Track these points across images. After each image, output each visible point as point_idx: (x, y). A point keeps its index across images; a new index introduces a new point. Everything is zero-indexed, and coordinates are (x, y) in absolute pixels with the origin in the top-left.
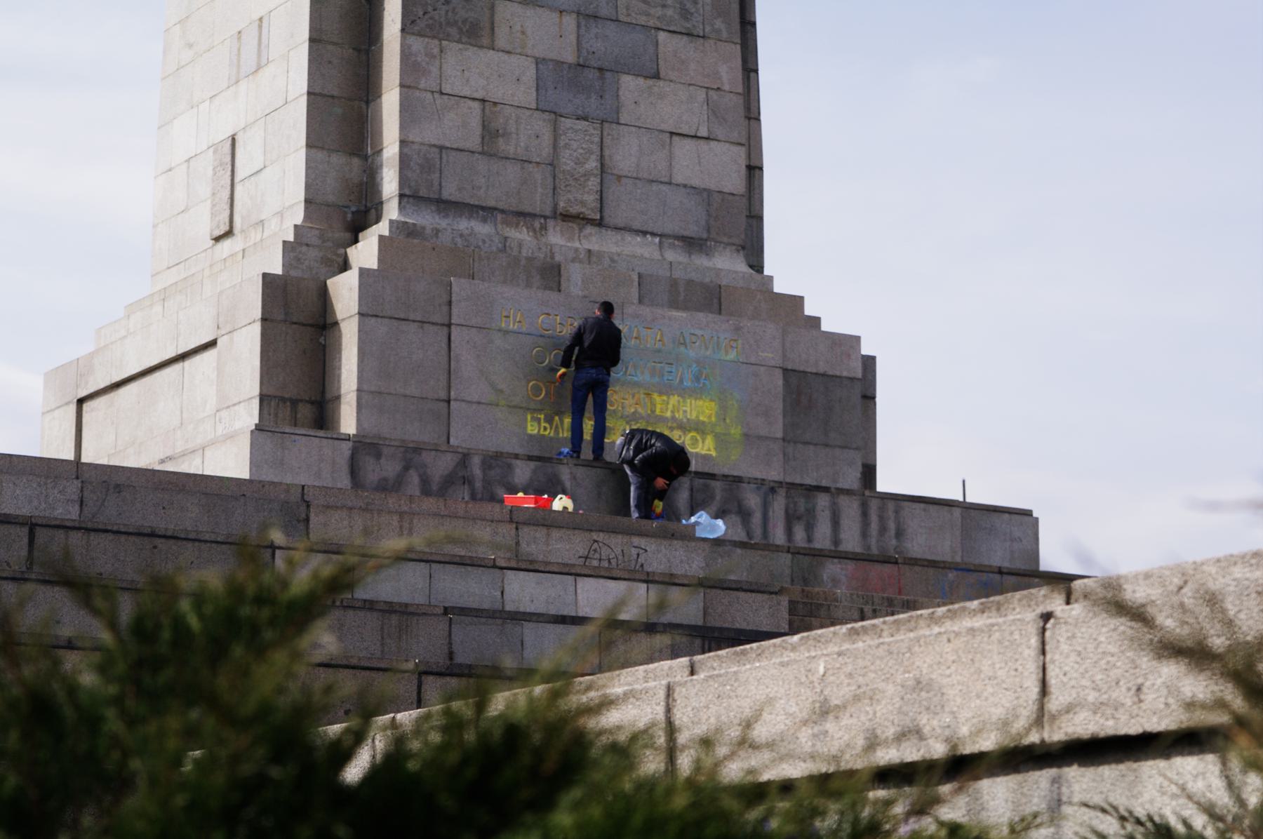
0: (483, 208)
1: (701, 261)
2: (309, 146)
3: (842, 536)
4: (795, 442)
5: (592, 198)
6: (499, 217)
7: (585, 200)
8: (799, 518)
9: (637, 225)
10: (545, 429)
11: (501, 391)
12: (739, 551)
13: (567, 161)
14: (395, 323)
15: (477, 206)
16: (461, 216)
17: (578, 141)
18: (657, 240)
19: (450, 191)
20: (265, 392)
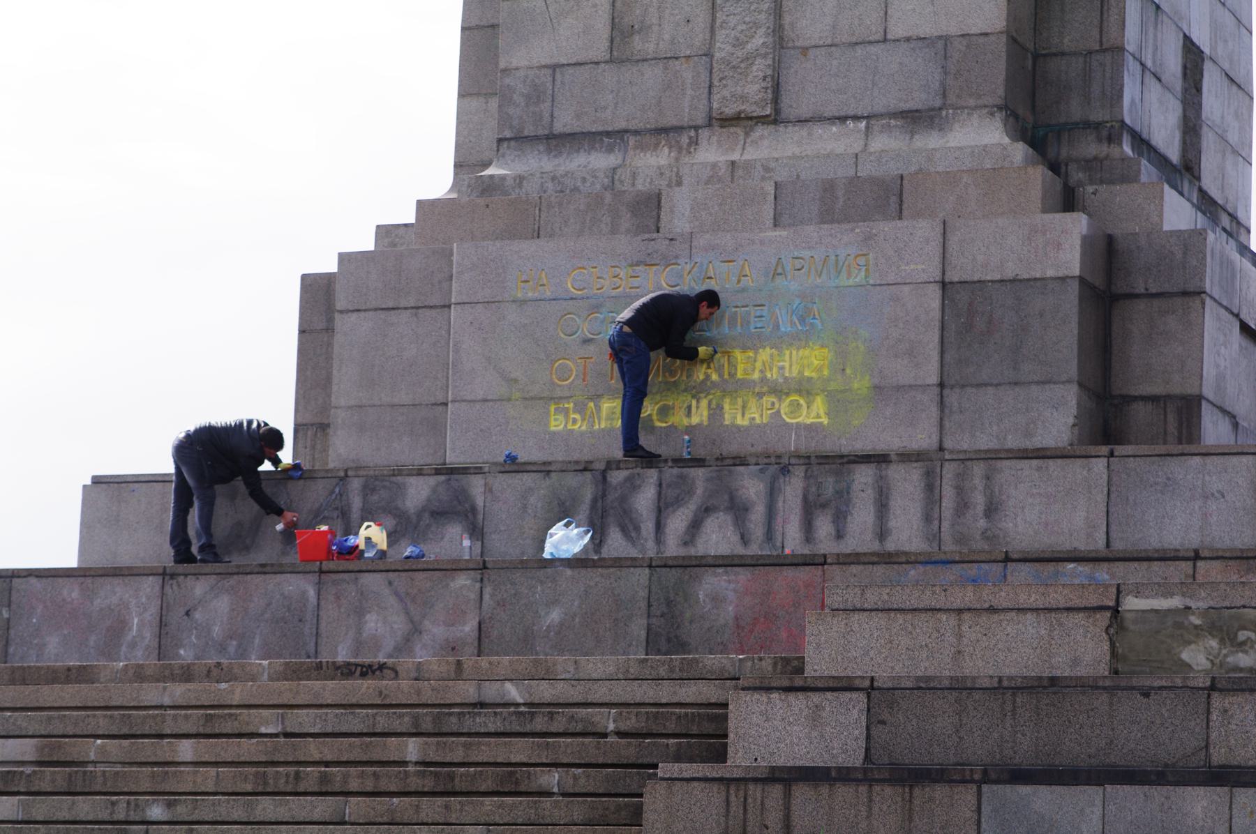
0: (608, 134)
1: (930, 141)
2: (461, 95)
3: (892, 523)
4: (963, 386)
5: (757, 87)
6: (632, 140)
7: (750, 91)
8: (824, 506)
9: (831, 111)
10: (575, 421)
11: (516, 381)
12: (569, 572)
13: (722, 49)
14: (383, 315)
15: (600, 133)
16: (578, 151)
18: (863, 124)
19: (565, 121)
20: (300, 420)
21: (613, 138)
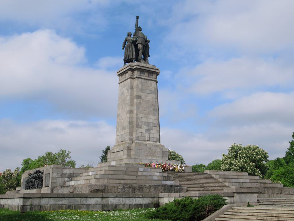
7: (148, 139)
17: (147, 135)
21: (142, 140)
